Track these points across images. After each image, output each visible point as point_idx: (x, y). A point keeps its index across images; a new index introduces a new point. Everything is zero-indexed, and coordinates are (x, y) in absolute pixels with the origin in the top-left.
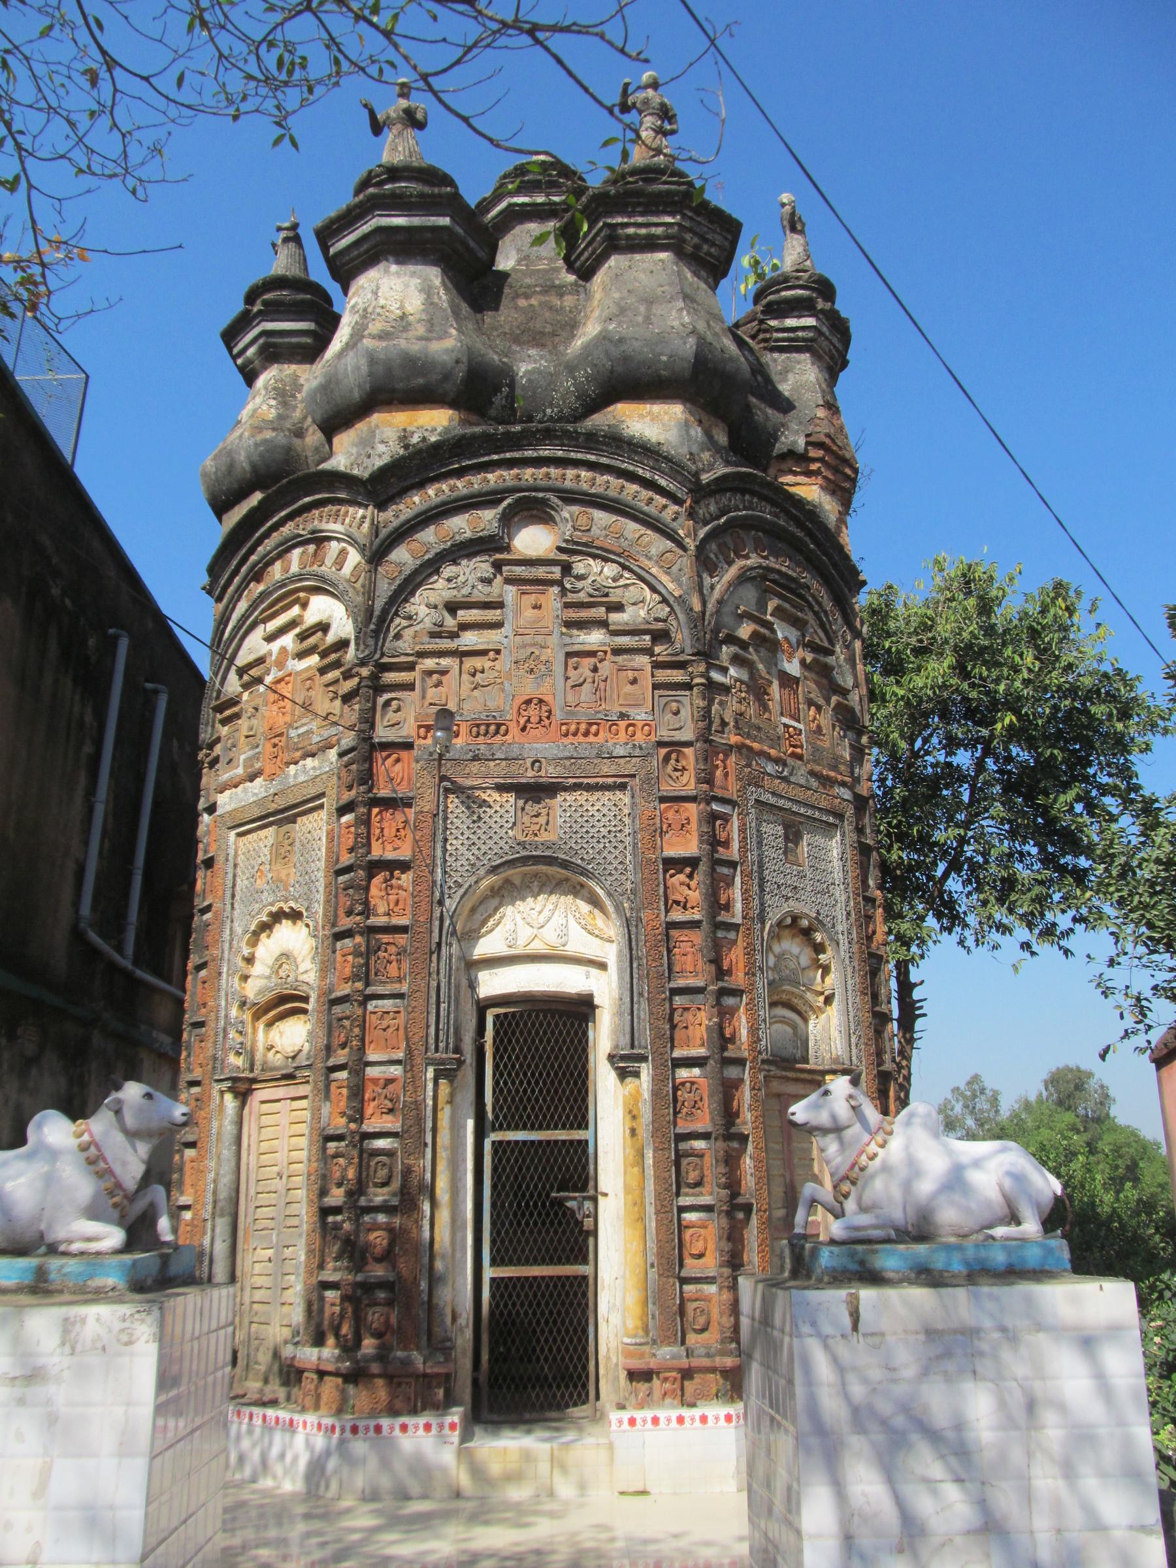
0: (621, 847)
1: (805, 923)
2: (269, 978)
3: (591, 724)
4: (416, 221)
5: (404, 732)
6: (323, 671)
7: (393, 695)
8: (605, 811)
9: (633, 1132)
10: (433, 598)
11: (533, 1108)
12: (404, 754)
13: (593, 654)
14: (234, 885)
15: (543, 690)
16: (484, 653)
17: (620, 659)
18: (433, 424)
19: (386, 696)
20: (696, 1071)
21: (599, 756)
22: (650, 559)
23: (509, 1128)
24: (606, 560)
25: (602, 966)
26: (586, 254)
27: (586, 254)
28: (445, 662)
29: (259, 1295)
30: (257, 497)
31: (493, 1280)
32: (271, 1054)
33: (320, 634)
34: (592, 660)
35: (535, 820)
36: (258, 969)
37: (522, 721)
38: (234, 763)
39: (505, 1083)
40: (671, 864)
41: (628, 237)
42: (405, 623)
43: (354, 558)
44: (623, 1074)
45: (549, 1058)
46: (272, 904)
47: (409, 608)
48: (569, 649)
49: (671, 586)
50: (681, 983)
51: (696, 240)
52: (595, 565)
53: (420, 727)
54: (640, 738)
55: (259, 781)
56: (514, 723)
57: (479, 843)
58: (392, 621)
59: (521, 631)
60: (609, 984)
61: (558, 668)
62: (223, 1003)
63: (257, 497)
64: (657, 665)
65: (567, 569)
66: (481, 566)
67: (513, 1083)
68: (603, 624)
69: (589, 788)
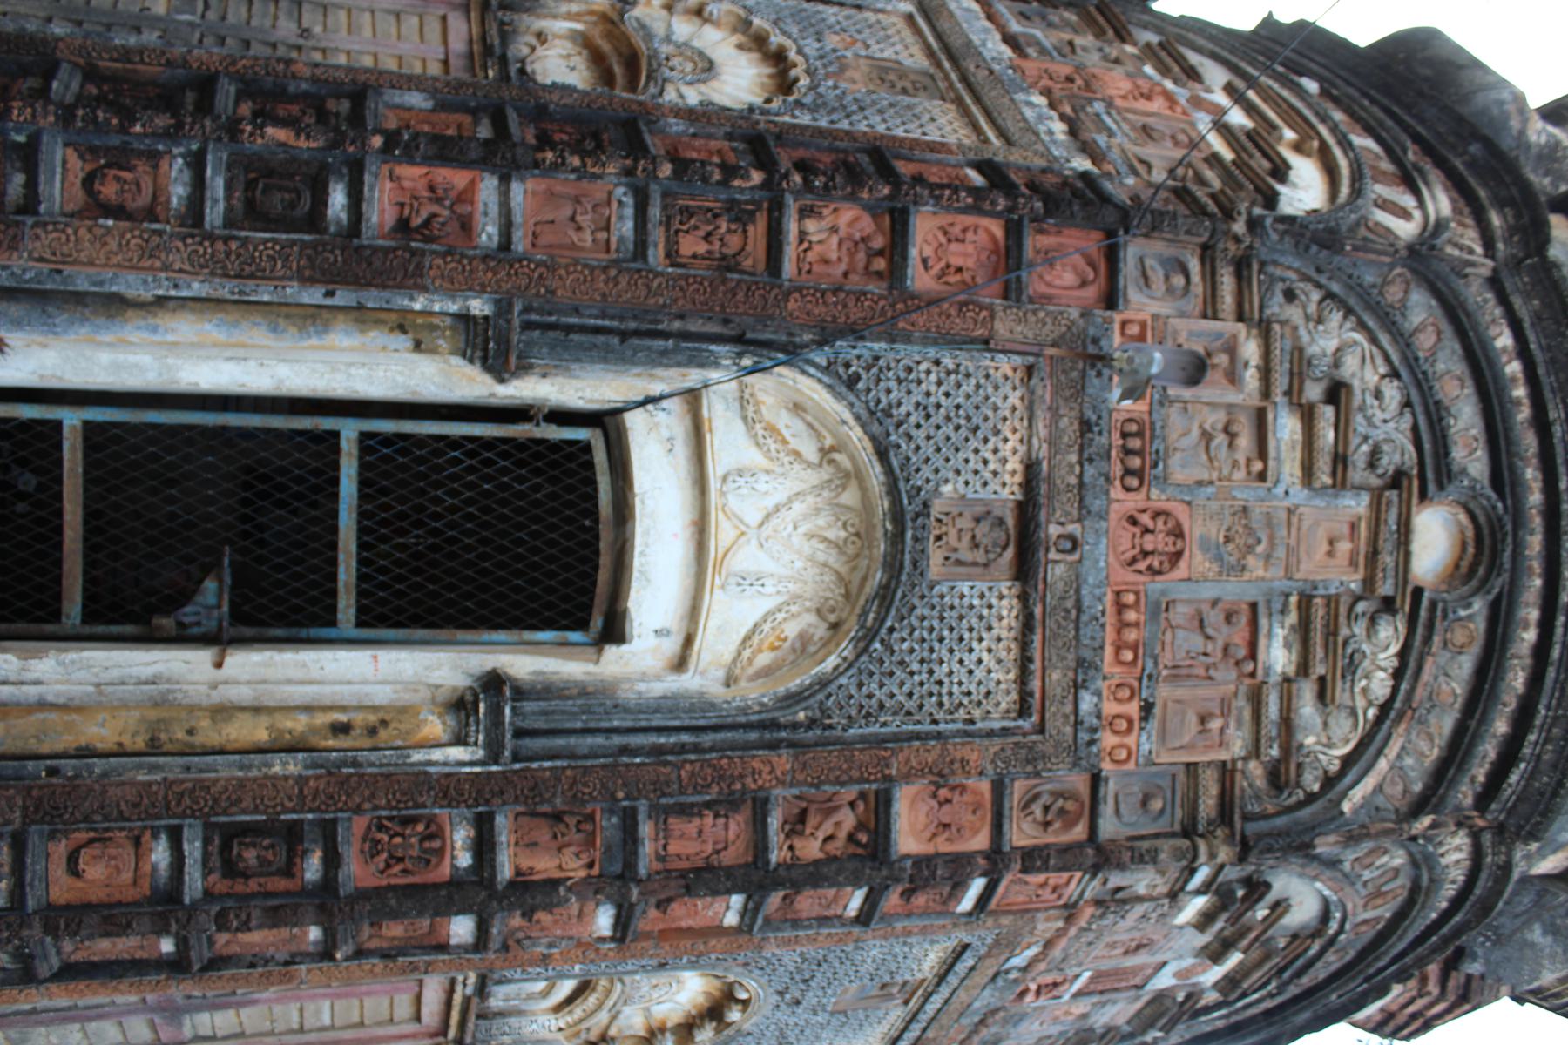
0: (911, 705)
1: (734, 1015)
2: (668, 39)
3: (1134, 648)
5: (1134, 295)
6: (1214, 159)
7: (1196, 277)
8: (979, 673)
9: (342, 729)
10: (1351, 364)
12: (1091, 293)
13: (1253, 655)
15: (1197, 561)
16: (1262, 452)
17: (1242, 705)
19: (1194, 265)
20: (465, 860)
21: (1080, 662)
22: (1399, 757)
23: (363, 466)
24: (1398, 675)
25: (680, 663)
28: (1251, 378)
31: (57, 425)
34: (1242, 652)
35: (966, 538)
36: (683, 28)
37: (1145, 519)
38: (1025, 22)
39: (456, 461)
40: (881, 805)
42: (1312, 308)
43: (1406, 230)
44: (461, 705)
45: (502, 550)
46: (800, 52)
47: (1337, 316)
48: (1262, 610)
49: (1358, 794)
50: (646, 829)
52: (1387, 657)
53: (1143, 325)
54: (1108, 740)
55: (1007, 52)
56: (1141, 505)
58: (1319, 286)
59: (1295, 520)
60: (644, 677)
61: (1235, 590)
64: (1226, 772)
65: (1388, 605)
66: (1400, 453)
67: (454, 478)
68: (1304, 668)
69: (1024, 644)
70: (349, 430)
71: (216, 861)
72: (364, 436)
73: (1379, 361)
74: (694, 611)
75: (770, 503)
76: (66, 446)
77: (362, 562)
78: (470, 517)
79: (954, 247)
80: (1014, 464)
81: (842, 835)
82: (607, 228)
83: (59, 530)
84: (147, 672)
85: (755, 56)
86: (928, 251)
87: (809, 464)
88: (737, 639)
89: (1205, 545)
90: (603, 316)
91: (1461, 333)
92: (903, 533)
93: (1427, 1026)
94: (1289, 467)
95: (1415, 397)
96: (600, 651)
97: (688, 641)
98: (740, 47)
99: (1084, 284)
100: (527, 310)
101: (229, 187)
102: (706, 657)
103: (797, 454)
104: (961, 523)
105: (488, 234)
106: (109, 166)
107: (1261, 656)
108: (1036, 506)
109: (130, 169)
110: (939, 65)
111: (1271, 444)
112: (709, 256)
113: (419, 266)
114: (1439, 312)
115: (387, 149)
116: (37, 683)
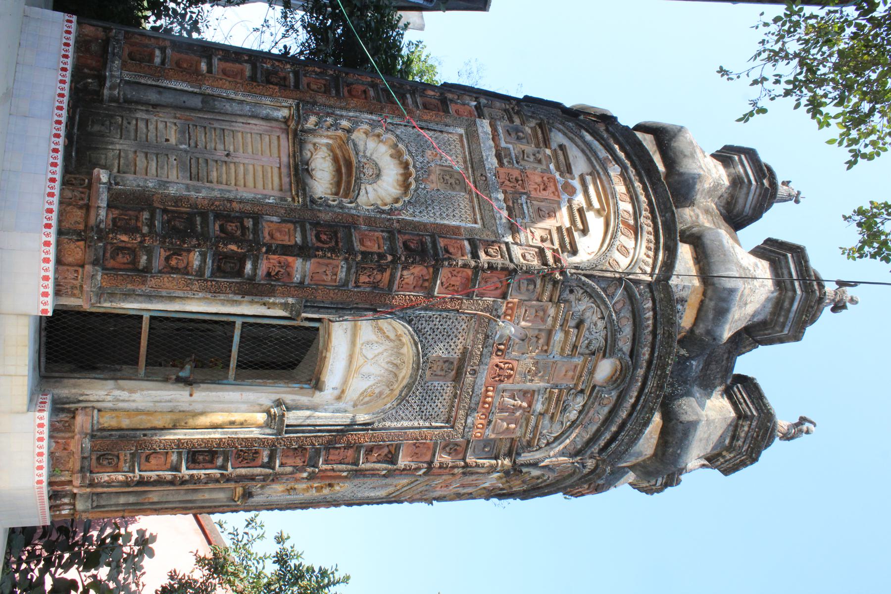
4: (792, 315)
8: (436, 409)
10: (588, 314)
11: (253, 348)
12: (499, 292)
14: (429, 130)
16: (548, 344)
18: (684, 318)
20: (266, 460)
24: (580, 412)
25: (339, 398)
26: (739, 396)
27: (739, 396)
28: (550, 321)
29: (141, 125)
30: (661, 168)
31: (141, 317)
32: (310, 146)
33: (581, 227)
35: (439, 368)
41: (742, 426)
51: (728, 458)
52: (578, 407)
55: (495, 161)
57: (433, 335)
58: (582, 288)
62: (351, 114)
63: (661, 168)
70: (239, 322)
71: (190, 459)
72: (244, 323)
73: (599, 313)
74: (345, 382)
75: (376, 352)
76: (144, 323)
77: (238, 361)
78: (276, 349)
79: (454, 278)
80: (460, 346)
81: (383, 454)
82: (336, 275)
83: (139, 348)
84: (169, 398)
85: (397, 162)
86: (444, 280)
87: (391, 340)
88: (359, 393)
89: (520, 374)
90: (332, 303)
91: (632, 304)
92: (418, 369)
93: (583, 495)
94: (557, 349)
95: (609, 326)
96: (314, 393)
97: (343, 392)
98: (391, 156)
99: (497, 288)
100: (307, 301)
101: (213, 262)
102: (348, 398)
103: (388, 337)
104: (438, 363)
105: (297, 278)
106: (174, 254)
107: (533, 407)
108: (465, 360)
109: (180, 255)
110: (467, 169)
111: (552, 341)
112: (369, 283)
113: (274, 290)
114: (626, 296)
115: (267, 252)
116: (134, 401)
